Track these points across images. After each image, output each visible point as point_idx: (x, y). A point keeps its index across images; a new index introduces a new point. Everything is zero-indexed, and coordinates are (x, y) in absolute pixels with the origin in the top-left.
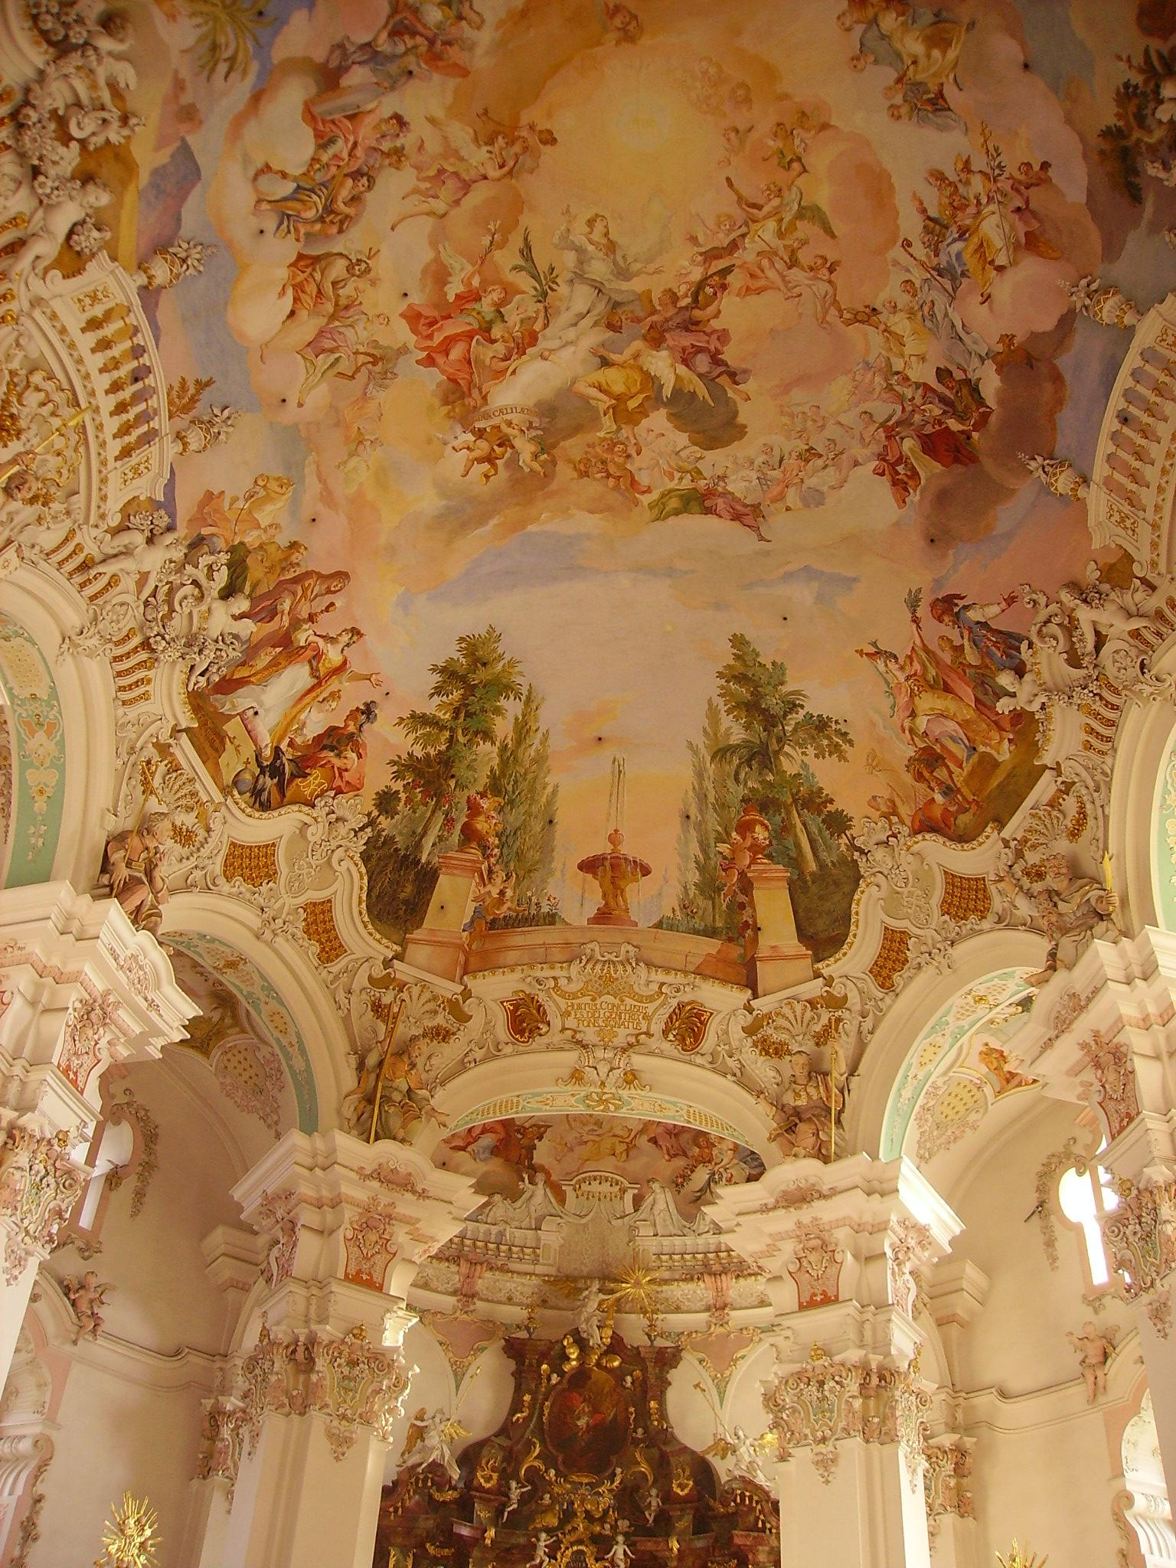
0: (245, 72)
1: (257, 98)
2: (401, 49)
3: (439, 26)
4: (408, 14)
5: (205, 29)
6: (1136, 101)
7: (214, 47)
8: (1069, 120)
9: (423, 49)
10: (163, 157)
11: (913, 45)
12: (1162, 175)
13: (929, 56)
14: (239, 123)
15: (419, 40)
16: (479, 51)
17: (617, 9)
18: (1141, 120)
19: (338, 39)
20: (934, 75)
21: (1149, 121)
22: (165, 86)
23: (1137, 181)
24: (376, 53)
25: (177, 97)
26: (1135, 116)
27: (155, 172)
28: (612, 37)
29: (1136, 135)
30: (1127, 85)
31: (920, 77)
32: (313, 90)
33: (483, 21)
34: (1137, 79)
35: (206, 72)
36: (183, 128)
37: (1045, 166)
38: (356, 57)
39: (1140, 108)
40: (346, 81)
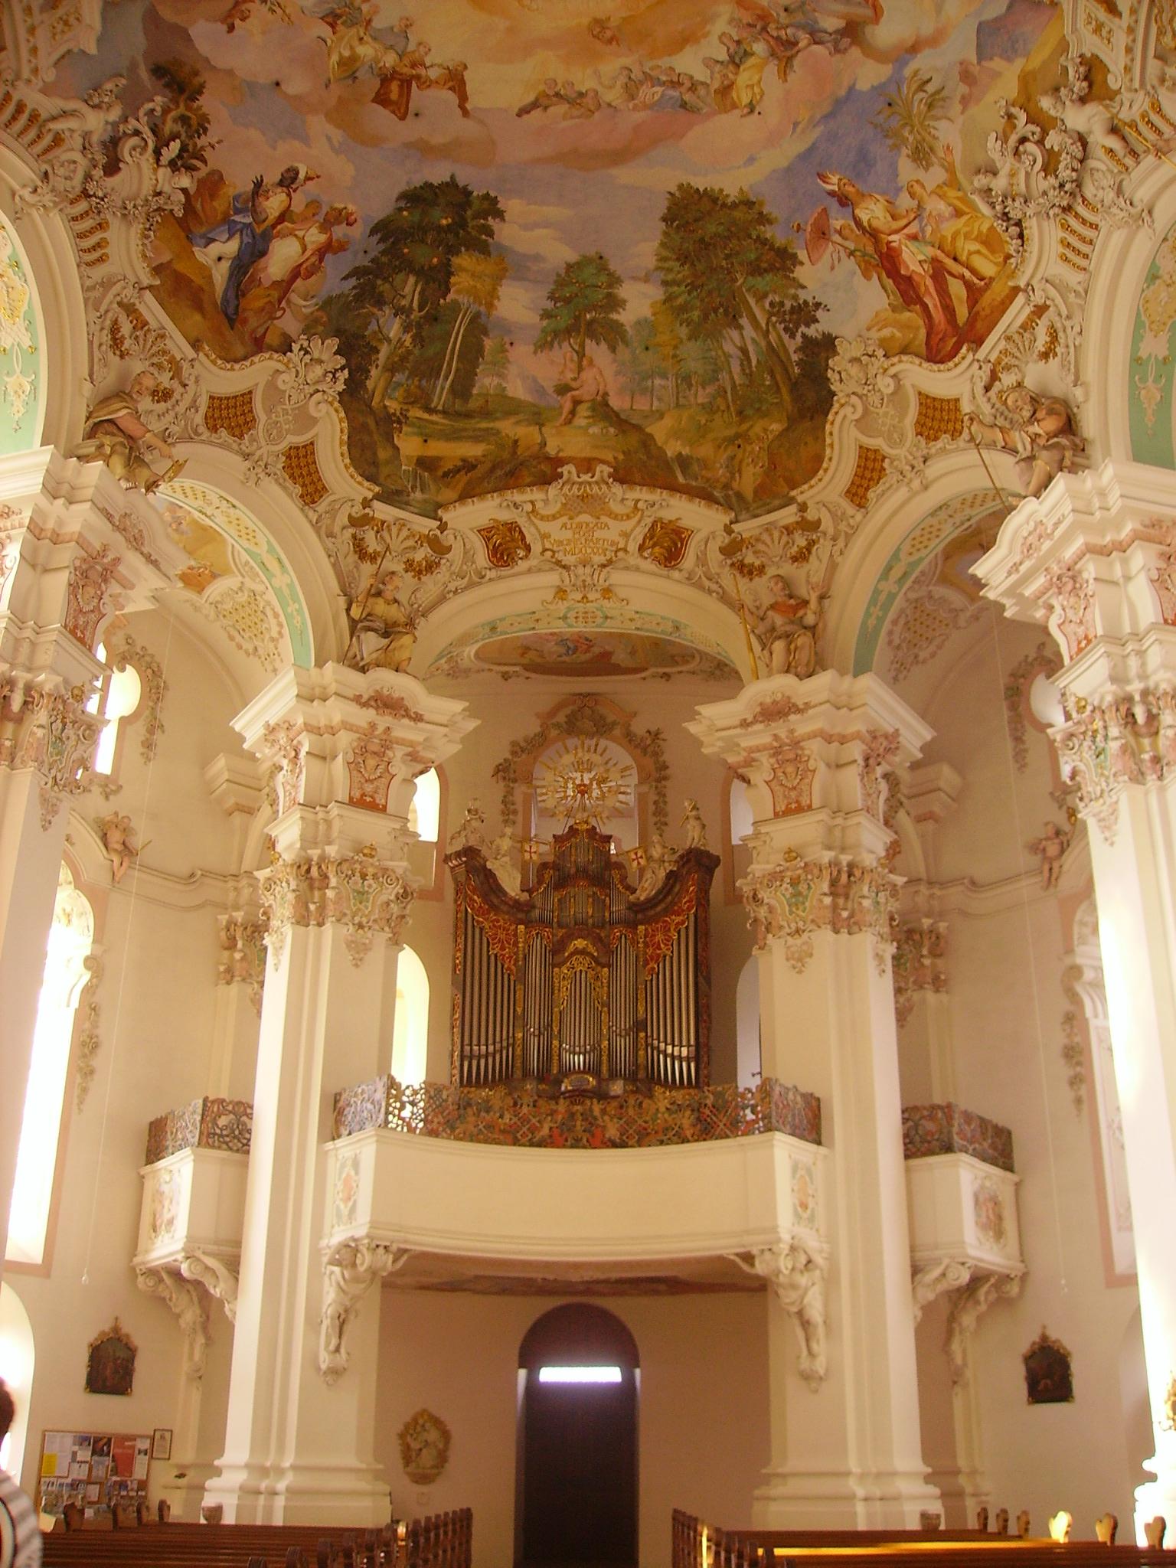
0: (916, 73)
1: (914, 49)
2: (789, 31)
3: (756, 40)
4: (780, 54)
5: (932, 123)
6: (194, 128)
7: (930, 106)
8: (230, 73)
9: (772, 26)
10: (997, 64)
11: (366, 51)
12: (151, 105)
13: (352, 48)
14: (934, 41)
15: (775, 34)
16: (726, 17)
17: (610, 41)
18: (184, 120)
19: (838, 56)
20: (342, 38)
21: (178, 128)
22: (973, 110)
23: (163, 82)
24: (811, 34)
25: (970, 95)
26: (189, 118)
27: (1009, 60)
28: (614, 22)
29: (182, 110)
30: (205, 130)
31: (353, 31)
32: (869, 30)
33: (720, 38)
34: (201, 142)
35: (944, 94)
36: (975, 70)
37: (231, 28)
38: (827, 37)
39: (190, 126)
40: (840, 24)
